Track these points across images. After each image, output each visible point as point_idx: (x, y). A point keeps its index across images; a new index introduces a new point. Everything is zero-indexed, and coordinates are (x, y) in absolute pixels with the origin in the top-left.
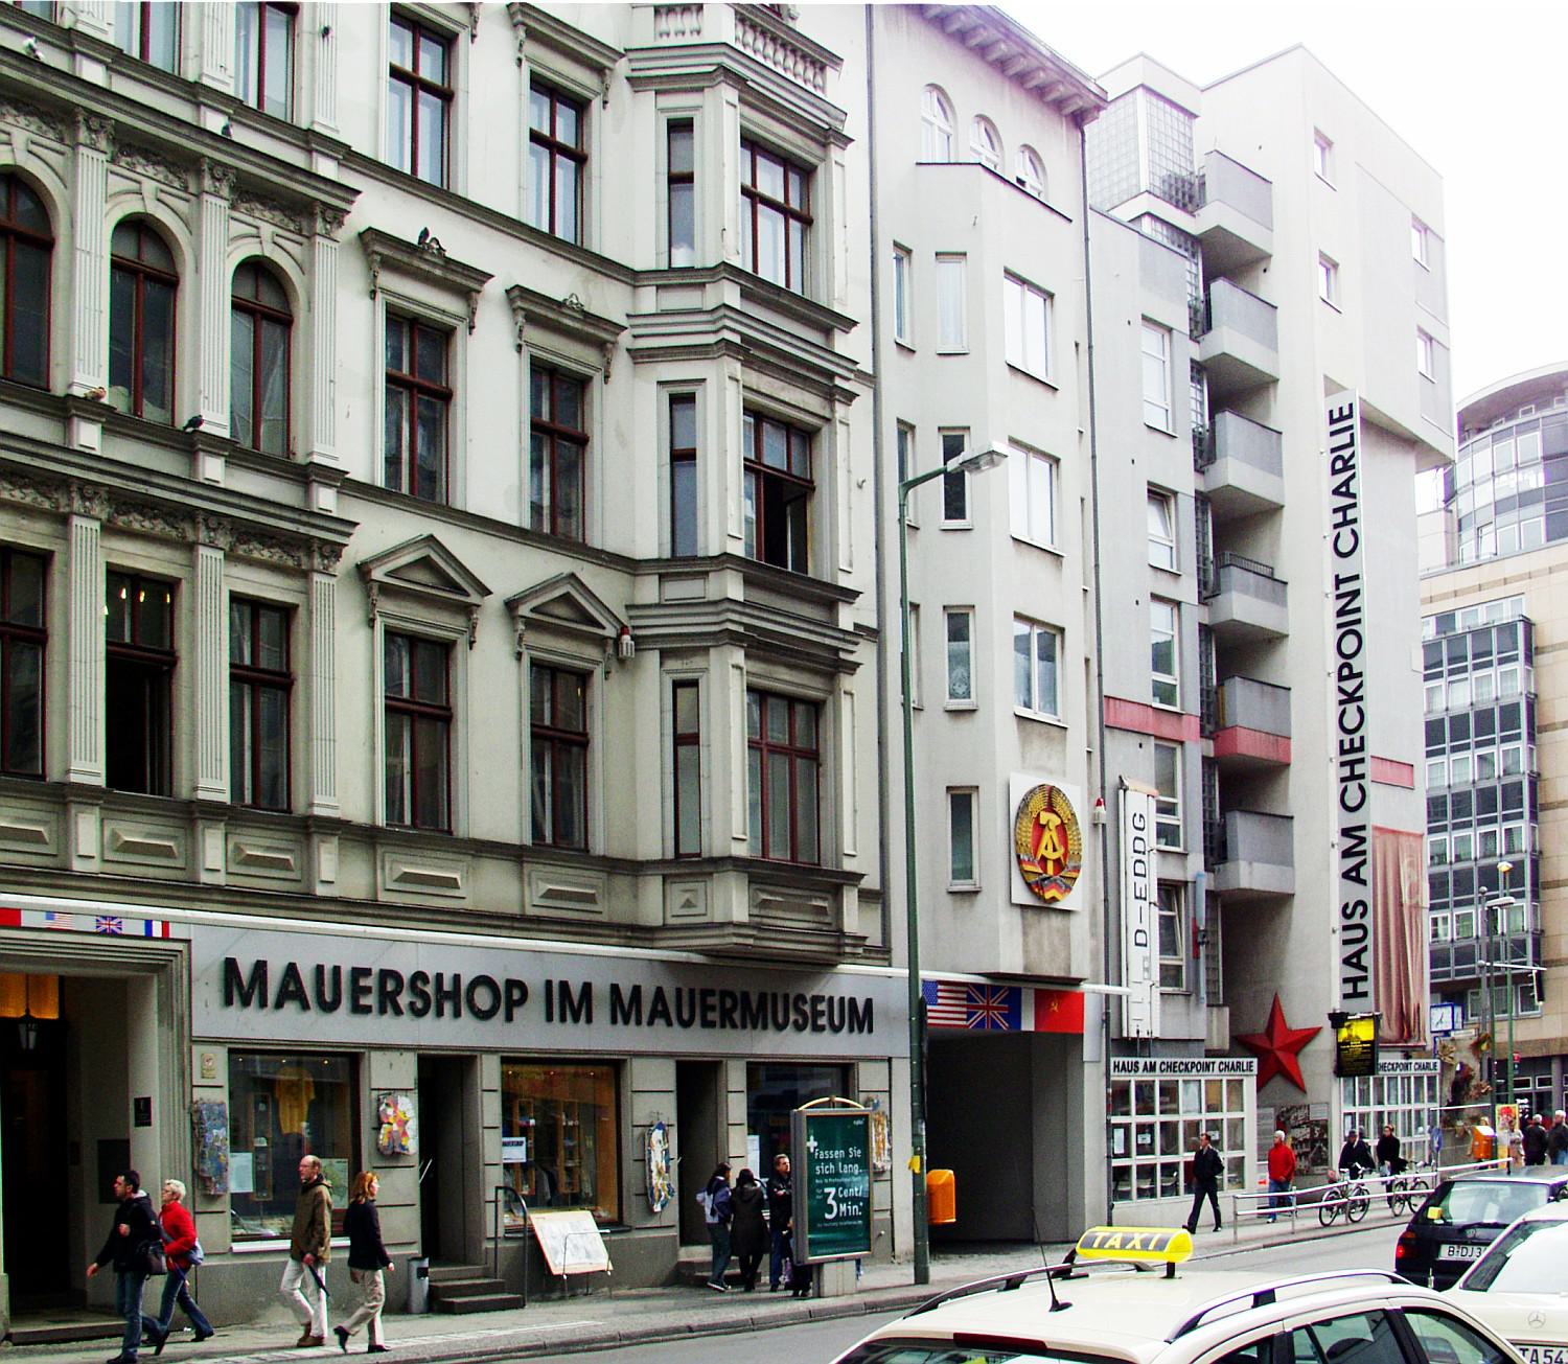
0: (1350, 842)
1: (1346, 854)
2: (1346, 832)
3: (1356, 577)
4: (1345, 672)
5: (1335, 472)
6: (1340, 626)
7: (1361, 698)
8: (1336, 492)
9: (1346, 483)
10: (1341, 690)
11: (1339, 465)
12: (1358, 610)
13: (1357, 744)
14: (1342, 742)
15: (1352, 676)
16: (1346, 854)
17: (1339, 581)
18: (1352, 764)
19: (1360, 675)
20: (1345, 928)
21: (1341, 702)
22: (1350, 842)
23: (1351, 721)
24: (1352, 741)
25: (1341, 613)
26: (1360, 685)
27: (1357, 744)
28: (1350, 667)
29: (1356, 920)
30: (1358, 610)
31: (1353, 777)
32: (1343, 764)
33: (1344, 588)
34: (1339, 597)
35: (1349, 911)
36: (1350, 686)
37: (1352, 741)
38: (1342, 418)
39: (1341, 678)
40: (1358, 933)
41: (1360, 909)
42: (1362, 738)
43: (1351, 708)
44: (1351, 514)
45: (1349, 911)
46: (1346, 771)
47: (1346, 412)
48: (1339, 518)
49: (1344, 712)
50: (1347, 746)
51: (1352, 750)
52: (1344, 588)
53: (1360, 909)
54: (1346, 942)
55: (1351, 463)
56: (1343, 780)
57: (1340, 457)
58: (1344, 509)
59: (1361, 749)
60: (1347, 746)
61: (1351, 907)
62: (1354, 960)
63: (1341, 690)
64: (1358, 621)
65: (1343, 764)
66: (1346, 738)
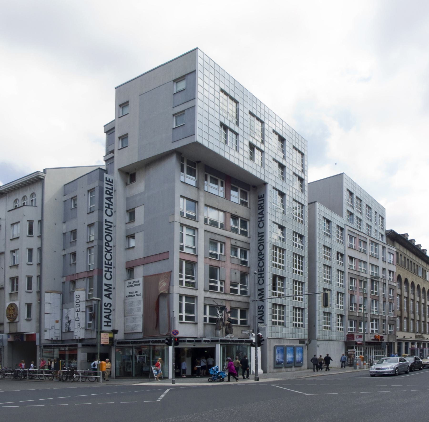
0: (260, 292)
1: (259, 295)
2: (259, 290)
3: (263, 233)
4: (260, 254)
5: (259, 209)
6: (259, 243)
7: (263, 260)
8: (259, 214)
9: (262, 212)
10: (259, 258)
11: (260, 208)
12: (263, 240)
13: (262, 270)
14: (259, 269)
15: (262, 255)
16: (259, 295)
17: (259, 233)
18: (261, 274)
19: (263, 254)
20: (259, 311)
21: (259, 260)
22: (260, 292)
23: (261, 264)
24: (261, 269)
25: (259, 240)
26: (263, 257)
27: (262, 270)
28: (261, 252)
29: (261, 310)
30: (263, 240)
31: (261, 277)
32: (259, 274)
33: (260, 235)
34: (259, 237)
35: (260, 308)
36: (261, 257)
37: (261, 269)
38: (261, 197)
39: (259, 255)
40: (261, 313)
41: (262, 307)
42: (263, 269)
43: (261, 262)
44: (263, 219)
45: (260, 308)
46: (260, 276)
47: (262, 196)
48: (260, 220)
49: (259, 263)
50: (260, 270)
51: (261, 271)
52: (260, 235)
53: (262, 307)
54: (259, 314)
55: (263, 207)
56: (259, 278)
57: (261, 206)
58: (261, 218)
59: (263, 271)
60: (260, 270)
61: (260, 306)
62: (261, 318)
63: (259, 258)
64: (263, 242)
65: (259, 274)
66: (260, 269)
